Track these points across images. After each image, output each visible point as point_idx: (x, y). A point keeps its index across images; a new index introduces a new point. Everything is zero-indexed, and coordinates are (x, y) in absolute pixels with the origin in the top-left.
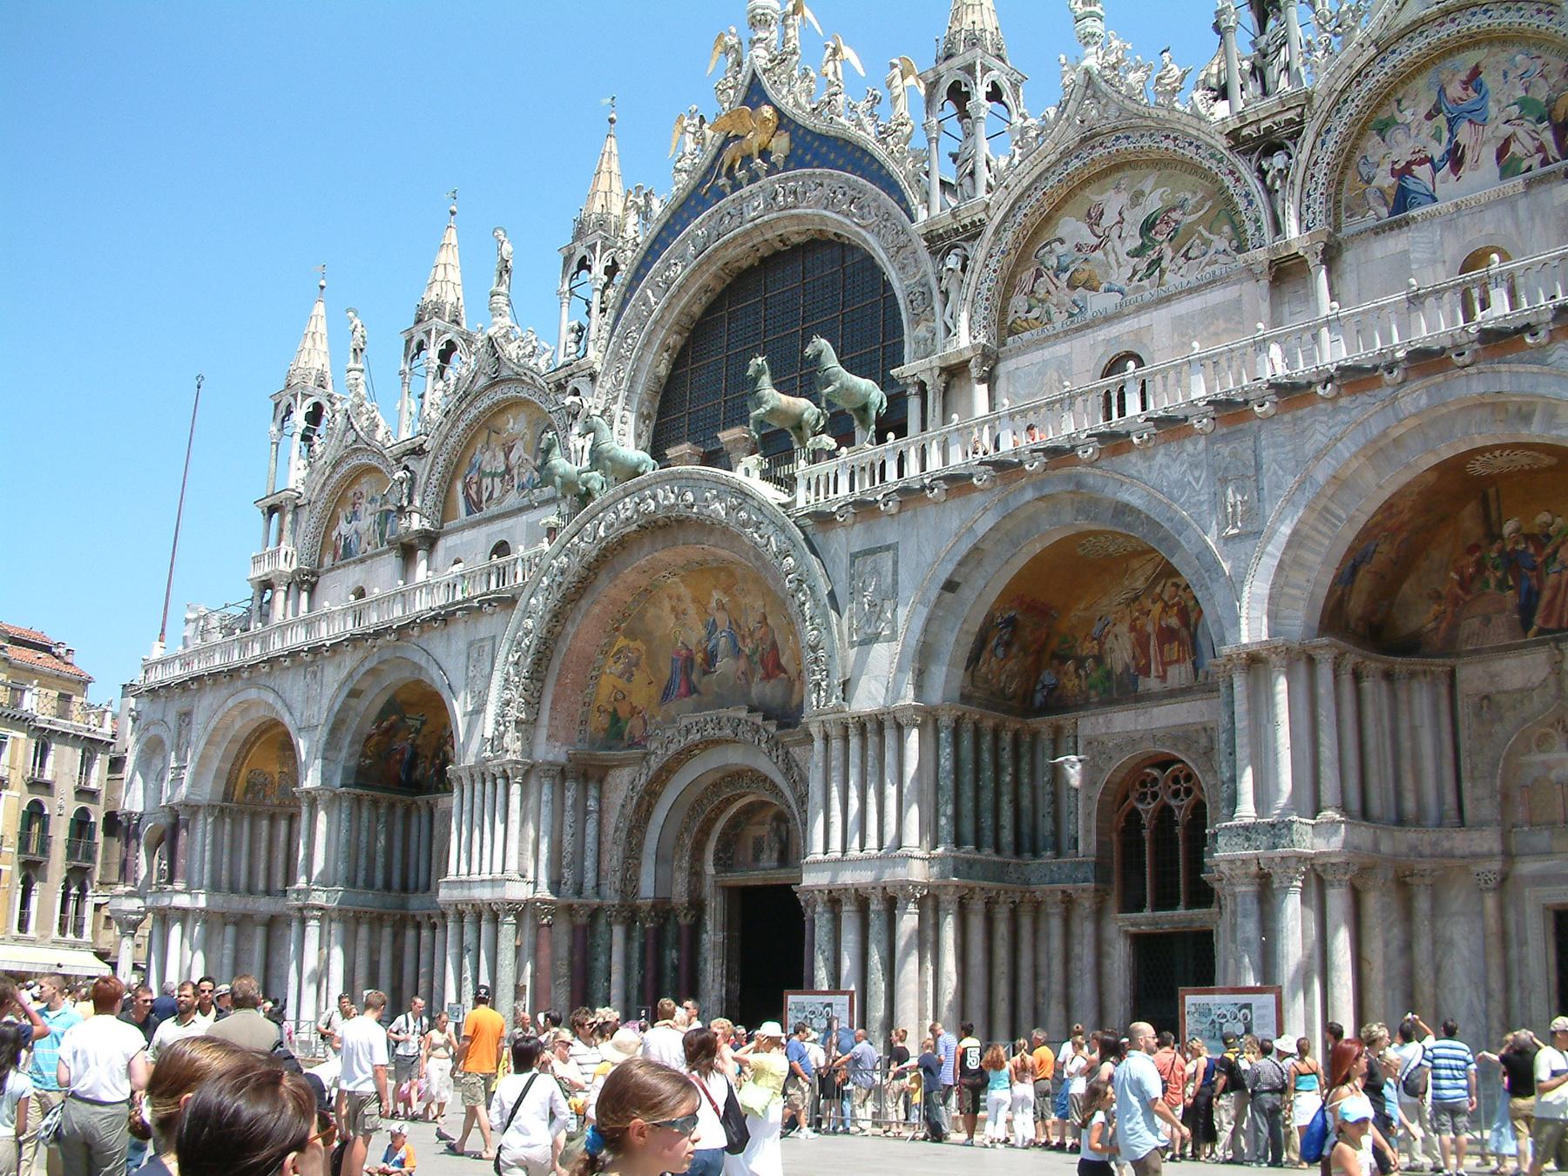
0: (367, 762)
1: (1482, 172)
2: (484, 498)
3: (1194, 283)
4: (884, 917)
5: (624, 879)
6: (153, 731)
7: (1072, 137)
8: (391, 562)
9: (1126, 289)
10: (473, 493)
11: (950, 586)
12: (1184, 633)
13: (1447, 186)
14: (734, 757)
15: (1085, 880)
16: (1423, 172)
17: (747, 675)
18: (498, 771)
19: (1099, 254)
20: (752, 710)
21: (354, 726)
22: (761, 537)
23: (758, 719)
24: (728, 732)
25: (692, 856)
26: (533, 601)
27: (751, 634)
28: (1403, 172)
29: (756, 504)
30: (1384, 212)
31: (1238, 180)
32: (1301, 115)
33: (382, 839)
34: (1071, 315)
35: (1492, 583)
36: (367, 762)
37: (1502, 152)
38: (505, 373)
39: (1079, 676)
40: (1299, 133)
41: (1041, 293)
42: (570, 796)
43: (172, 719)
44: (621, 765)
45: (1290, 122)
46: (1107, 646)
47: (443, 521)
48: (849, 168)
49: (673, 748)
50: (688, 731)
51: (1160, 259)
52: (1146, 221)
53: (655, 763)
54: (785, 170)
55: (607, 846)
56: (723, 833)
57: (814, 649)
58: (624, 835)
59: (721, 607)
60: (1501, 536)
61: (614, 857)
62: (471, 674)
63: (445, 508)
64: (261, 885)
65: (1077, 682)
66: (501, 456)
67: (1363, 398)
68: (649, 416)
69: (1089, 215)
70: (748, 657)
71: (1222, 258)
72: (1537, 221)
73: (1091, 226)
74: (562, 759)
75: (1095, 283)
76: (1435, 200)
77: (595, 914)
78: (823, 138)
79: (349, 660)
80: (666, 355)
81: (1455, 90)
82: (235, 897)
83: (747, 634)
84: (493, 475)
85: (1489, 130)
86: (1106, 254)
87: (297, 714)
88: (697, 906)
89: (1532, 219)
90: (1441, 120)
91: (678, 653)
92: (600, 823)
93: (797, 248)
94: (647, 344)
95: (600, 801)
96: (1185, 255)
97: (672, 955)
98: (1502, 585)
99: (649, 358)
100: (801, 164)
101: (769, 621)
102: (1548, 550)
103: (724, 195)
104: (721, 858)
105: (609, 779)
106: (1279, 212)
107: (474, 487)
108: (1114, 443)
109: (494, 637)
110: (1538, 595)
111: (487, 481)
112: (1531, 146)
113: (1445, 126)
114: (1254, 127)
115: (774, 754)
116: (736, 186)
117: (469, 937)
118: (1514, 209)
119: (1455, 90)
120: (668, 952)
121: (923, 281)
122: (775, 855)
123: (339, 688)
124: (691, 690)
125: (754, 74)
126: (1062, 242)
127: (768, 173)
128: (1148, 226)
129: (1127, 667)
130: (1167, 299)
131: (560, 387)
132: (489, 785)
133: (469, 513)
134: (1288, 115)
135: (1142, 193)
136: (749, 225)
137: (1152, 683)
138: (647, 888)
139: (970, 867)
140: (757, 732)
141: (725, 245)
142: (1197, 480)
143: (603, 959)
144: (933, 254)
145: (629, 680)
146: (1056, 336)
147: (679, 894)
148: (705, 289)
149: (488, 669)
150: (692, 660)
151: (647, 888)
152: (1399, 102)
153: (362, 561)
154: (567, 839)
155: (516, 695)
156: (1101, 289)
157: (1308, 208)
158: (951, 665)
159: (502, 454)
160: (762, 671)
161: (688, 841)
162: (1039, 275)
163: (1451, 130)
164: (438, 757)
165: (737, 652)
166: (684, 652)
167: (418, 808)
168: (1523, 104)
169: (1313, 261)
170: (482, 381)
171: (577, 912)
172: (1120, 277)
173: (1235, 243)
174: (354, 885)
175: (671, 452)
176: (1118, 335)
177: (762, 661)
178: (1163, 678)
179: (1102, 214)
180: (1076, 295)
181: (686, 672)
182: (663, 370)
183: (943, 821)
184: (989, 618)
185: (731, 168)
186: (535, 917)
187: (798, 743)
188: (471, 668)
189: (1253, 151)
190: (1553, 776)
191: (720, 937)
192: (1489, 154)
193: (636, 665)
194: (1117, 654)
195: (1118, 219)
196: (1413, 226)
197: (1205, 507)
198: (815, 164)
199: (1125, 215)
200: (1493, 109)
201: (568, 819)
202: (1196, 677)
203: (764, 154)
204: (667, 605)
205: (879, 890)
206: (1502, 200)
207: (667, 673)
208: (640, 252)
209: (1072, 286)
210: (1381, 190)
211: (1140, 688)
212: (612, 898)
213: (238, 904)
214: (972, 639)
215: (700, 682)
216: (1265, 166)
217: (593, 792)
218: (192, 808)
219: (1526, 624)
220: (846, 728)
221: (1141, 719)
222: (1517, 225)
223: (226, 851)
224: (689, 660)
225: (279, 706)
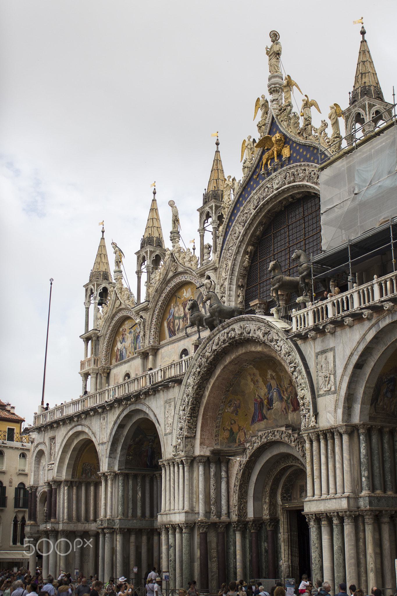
0: (130, 457)
4: (339, 527)
5: (239, 509)
6: (40, 447)
8: (138, 361)
11: (359, 366)
14: (283, 450)
17: (286, 409)
18: (179, 460)
21: (122, 441)
22: (278, 346)
23: (290, 432)
25: (270, 497)
26: (189, 381)
27: (286, 390)
29: (275, 331)
33: (140, 494)
36: (130, 457)
38: (180, 270)
42: (212, 470)
43: (47, 441)
44: (235, 454)
47: (160, 341)
50: (261, 438)
53: (249, 453)
54: (289, 164)
55: (232, 493)
56: (285, 485)
57: (303, 398)
58: (238, 488)
59: (272, 378)
61: (234, 499)
62: (167, 416)
63: (160, 335)
64: (92, 518)
66: (182, 309)
68: (242, 286)
74: (208, 454)
77: (228, 525)
78: (304, 146)
79: (117, 412)
80: (247, 256)
82: (80, 524)
84: (179, 318)
87: (98, 437)
88: (275, 521)
91: (256, 400)
92: (228, 483)
93: (299, 200)
95: (227, 472)
97: (265, 545)
99: (239, 258)
103: (264, 178)
104: (284, 497)
107: (172, 324)
111: (177, 321)
115: (297, 448)
116: (269, 174)
117: (171, 541)
120: (263, 544)
123: (114, 424)
124: (264, 418)
125: (273, 118)
127: (282, 166)
131: (202, 275)
133: (170, 337)
136: (275, 192)
139: (379, 501)
140: (290, 436)
141: (268, 202)
143: (232, 548)
145: (236, 414)
147: (266, 515)
148: (260, 223)
150: (263, 404)
151: (251, 515)
153: (128, 361)
154: (212, 491)
155: (184, 425)
158: (363, 403)
159: (182, 308)
160: (292, 407)
161: (268, 489)
165: (281, 399)
167: (156, 477)
170: (171, 274)
171: (219, 526)
174: (128, 516)
175: (252, 304)
182: (246, 264)
183: (364, 479)
184: (380, 379)
188: (166, 413)
191: (286, 536)
193: (239, 407)
201: (212, 482)
203: (280, 156)
204: (249, 378)
205: (335, 514)
208: (231, 208)
212: (234, 518)
213: (81, 527)
214: (372, 391)
215: (267, 414)
217: (224, 468)
218: (58, 483)
220: (318, 436)
223: (74, 502)
224: (262, 402)
225: (90, 434)
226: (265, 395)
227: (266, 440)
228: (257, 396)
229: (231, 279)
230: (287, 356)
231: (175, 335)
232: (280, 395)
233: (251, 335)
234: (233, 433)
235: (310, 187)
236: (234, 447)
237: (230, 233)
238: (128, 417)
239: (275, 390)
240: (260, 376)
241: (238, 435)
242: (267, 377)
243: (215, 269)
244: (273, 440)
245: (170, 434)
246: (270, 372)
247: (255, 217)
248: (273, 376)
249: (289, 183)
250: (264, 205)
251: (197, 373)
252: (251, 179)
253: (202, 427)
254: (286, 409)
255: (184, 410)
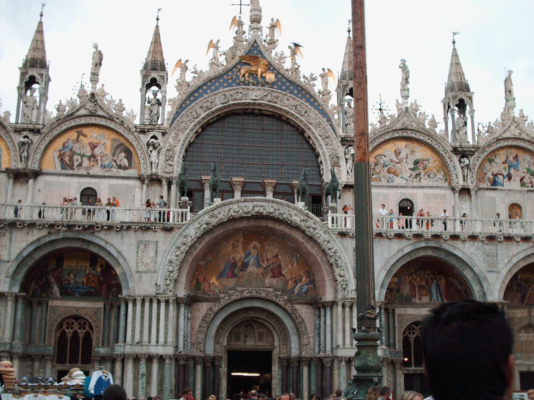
1: (515, 184)
2: (76, 164)
3: (431, 185)
7: (399, 126)
9: (408, 180)
10: (67, 159)
12: (427, 287)
13: (507, 185)
15: (400, 357)
16: (501, 177)
18: (162, 299)
19: (398, 165)
20: (276, 290)
24: (263, 295)
28: (495, 175)
30: (489, 184)
31: (451, 161)
32: (475, 151)
34: (388, 181)
35: (515, 290)
37: (522, 180)
38: (100, 113)
39: (391, 295)
40: (473, 155)
41: (378, 171)
45: (472, 151)
46: (401, 287)
48: (304, 99)
49: (234, 298)
51: (419, 174)
52: (416, 161)
53: (223, 303)
57: (341, 276)
59: (255, 247)
60: (517, 279)
62: (140, 255)
65: (390, 296)
67: (525, 244)
69: (395, 151)
70: (264, 268)
71: (440, 181)
72: (529, 201)
73: (396, 155)
75: (397, 174)
76: (503, 186)
78: (290, 82)
81: (511, 159)
83: (265, 259)
84: (82, 156)
85: (519, 173)
86: (402, 166)
89: (528, 200)
90: (506, 165)
91: (229, 261)
94: (192, 130)
96: (428, 176)
98: (517, 291)
100: (280, 88)
101: (279, 257)
102: (529, 284)
103: (239, 84)
105: (194, 306)
106: (466, 176)
108: (455, 237)
109: (157, 242)
110: (526, 295)
111: (75, 157)
112: (529, 181)
113: (507, 168)
114: (462, 149)
118: (523, 195)
119: (511, 159)
121: (336, 152)
122: (253, 340)
124: (234, 276)
126: (385, 157)
128: (416, 163)
129: (408, 295)
130: (423, 187)
131: (143, 132)
132: (155, 305)
133: (63, 168)
134: (473, 150)
135: (414, 152)
137: (417, 300)
138: (210, 351)
140: (277, 296)
142: (479, 254)
144: (343, 145)
146: (383, 186)
148: (218, 116)
149: (152, 254)
152: (495, 156)
156: (399, 176)
157: (472, 177)
160: (271, 274)
162: (376, 164)
163: (509, 169)
164: (42, 281)
165: (259, 266)
166: (232, 261)
168: (528, 170)
169: (473, 193)
170: (83, 112)
172: (407, 175)
173: (444, 178)
176: (407, 193)
177: (272, 271)
178: (420, 299)
179: (400, 153)
180: (391, 175)
181: (232, 268)
185: (244, 75)
186: (177, 360)
187: (298, 304)
188: (140, 252)
189: (459, 154)
190: (521, 339)
192: (518, 179)
194: (405, 290)
195: (406, 156)
196: (497, 191)
197: (482, 262)
198: (288, 91)
199: (408, 156)
200: (520, 168)
202: (431, 301)
204: (232, 242)
206: (520, 191)
207: (222, 266)
209: (389, 171)
210: (489, 178)
211: (413, 301)
215: (239, 273)
216: (462, 160)
219: (523, 302)
221: (417, 311)
222: (524, 200)
226: (241, 258)
227: (248, 295)
228: (231, 258)
229: (182, 149)
230: (325, 243)
231: (74, 169)
232: (258, 262)
233: (284, 216)
234: (199, 282)
235: (293, 115)
236: (199, 294)
237: (187, 109)
238: (52, 242)
239: (253, 257)
240: (243, 243)
241: (203, 285)
242: (249, 246)
243: (164, 134)
244: (257, 296)
245: (146, 272)
246: (254, 243)
247: (220, 109)
248: (256, 247)
249: (269, 102)
250: (233, 104)
251: (202, 227)
252: (221, 76)
253: (187, 273)
254: (264, 275)
255: (177, 256)
